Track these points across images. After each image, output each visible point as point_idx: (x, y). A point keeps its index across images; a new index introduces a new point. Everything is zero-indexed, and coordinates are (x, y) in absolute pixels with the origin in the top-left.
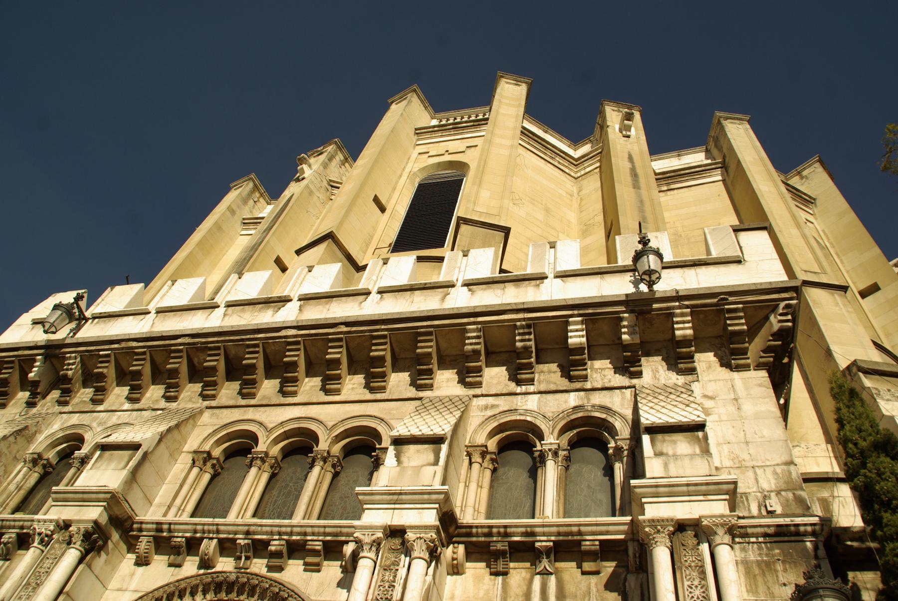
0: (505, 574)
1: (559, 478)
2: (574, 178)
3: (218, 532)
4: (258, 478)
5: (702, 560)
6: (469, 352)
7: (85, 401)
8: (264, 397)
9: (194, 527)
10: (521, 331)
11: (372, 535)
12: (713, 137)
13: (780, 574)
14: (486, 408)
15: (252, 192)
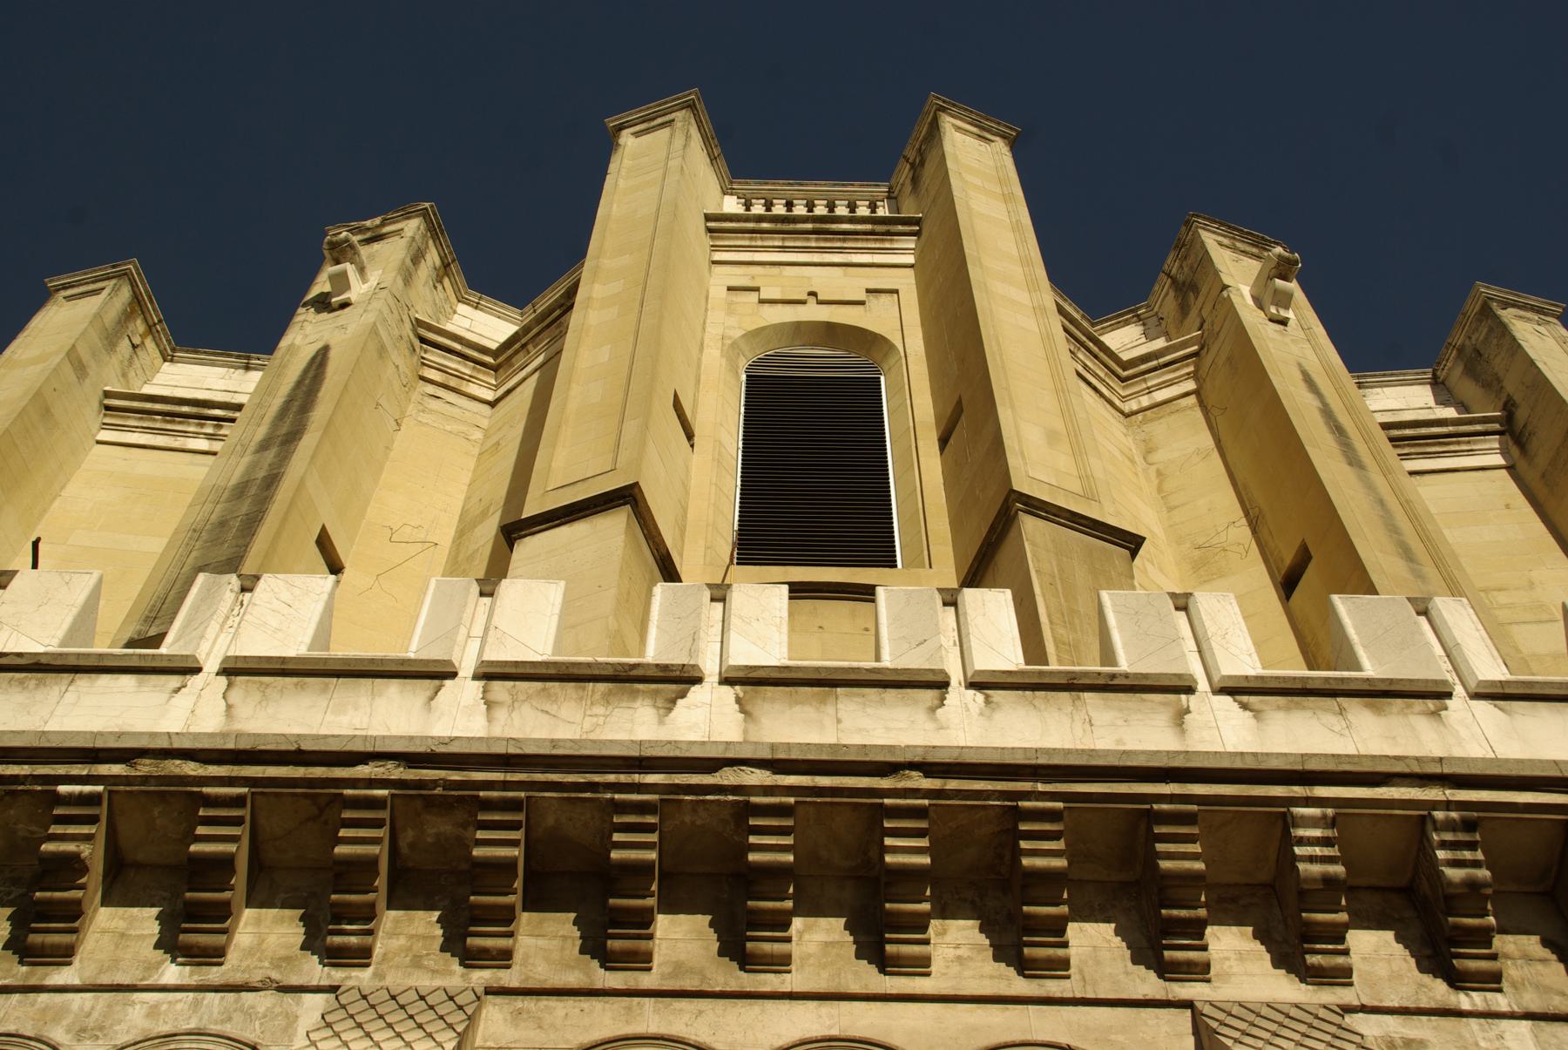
2: (1122, 412)
6: (1314, 880)
8: (678, 968)
10: (1449, 837)
15: (127, 316)
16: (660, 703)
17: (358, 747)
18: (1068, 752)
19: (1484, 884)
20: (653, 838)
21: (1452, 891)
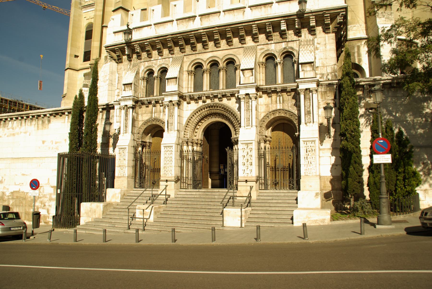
0: (271, 97)
1: (282, 69)
3: (205, 95)
4: (207, 76)
5: (310, 97)
7: (146, 58)
8: (199, 50)
10: (268, 26)
13: (328, 94)
14: (261, 49)
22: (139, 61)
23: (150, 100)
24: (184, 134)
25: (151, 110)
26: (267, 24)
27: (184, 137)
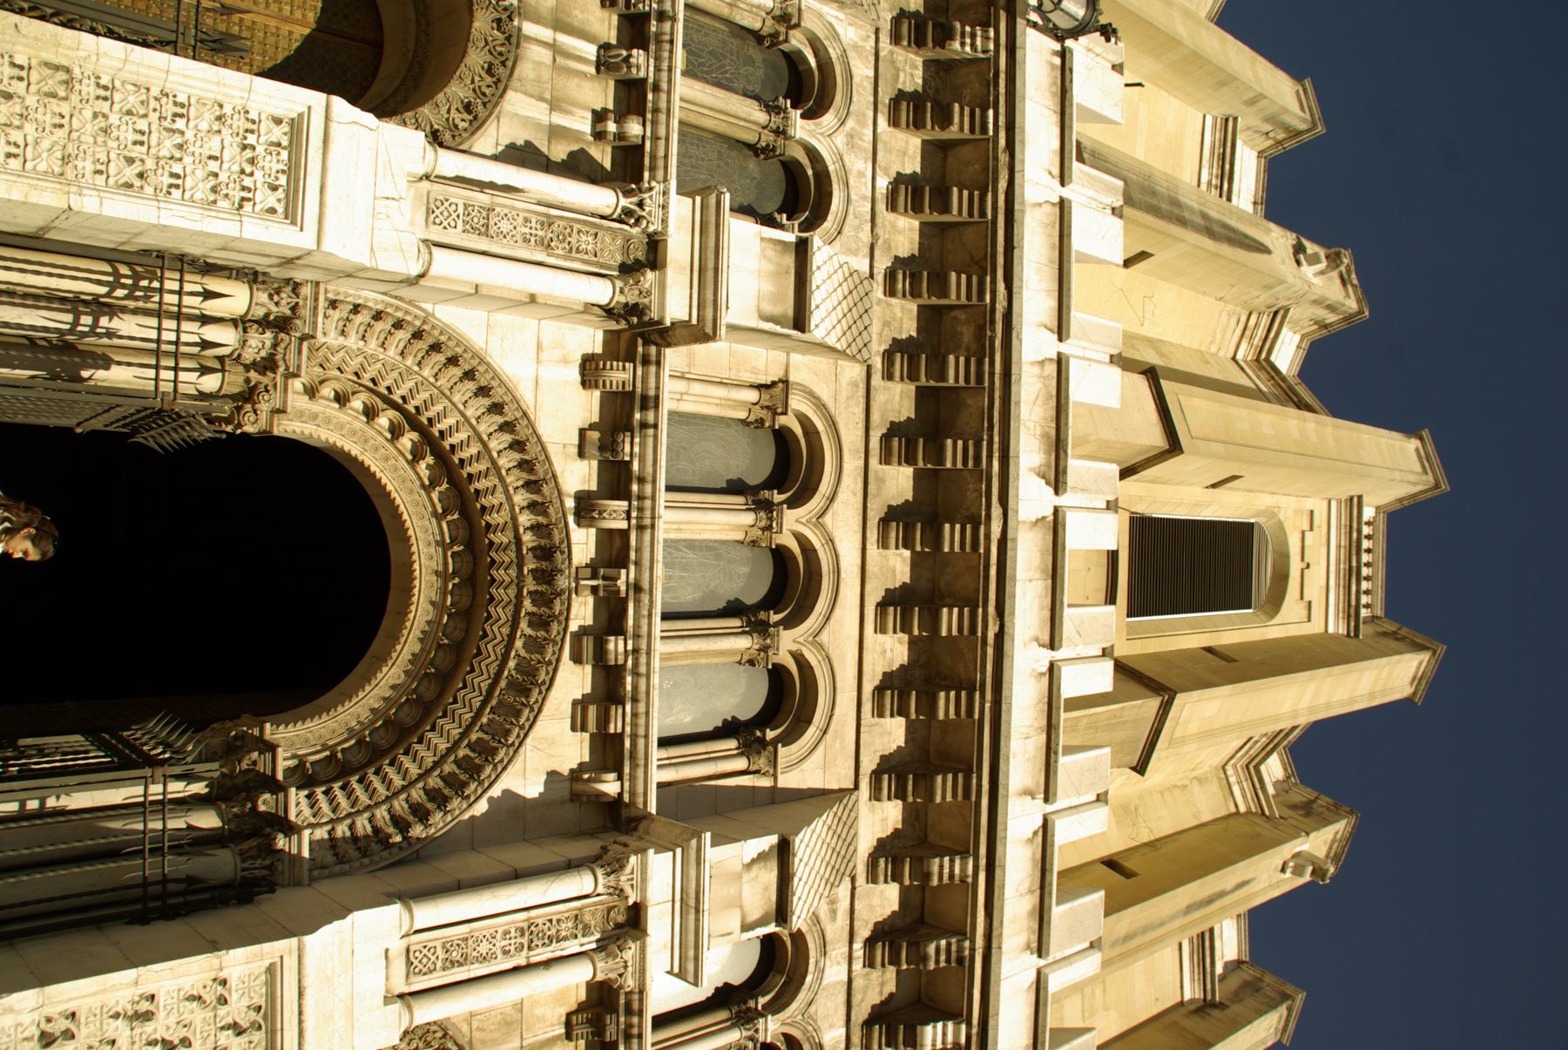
3: (641, 528)
6: (929, 866)
7: (896, 78)
8: (881, 481)
9: (650, 478)
10: (954, 948)
11: (632, 886)
12: (1260, 980)
16: (1043, 469)
17: (1016, 283)
18: (1009, 723)
19: (925, 966)
20: (959, 465)
21: (922, 945)
22: (887, 17)
23: (659, 42)
24: (356, 309)
25: (578, 17)
26: (967, 944)
27: (333, 304)
